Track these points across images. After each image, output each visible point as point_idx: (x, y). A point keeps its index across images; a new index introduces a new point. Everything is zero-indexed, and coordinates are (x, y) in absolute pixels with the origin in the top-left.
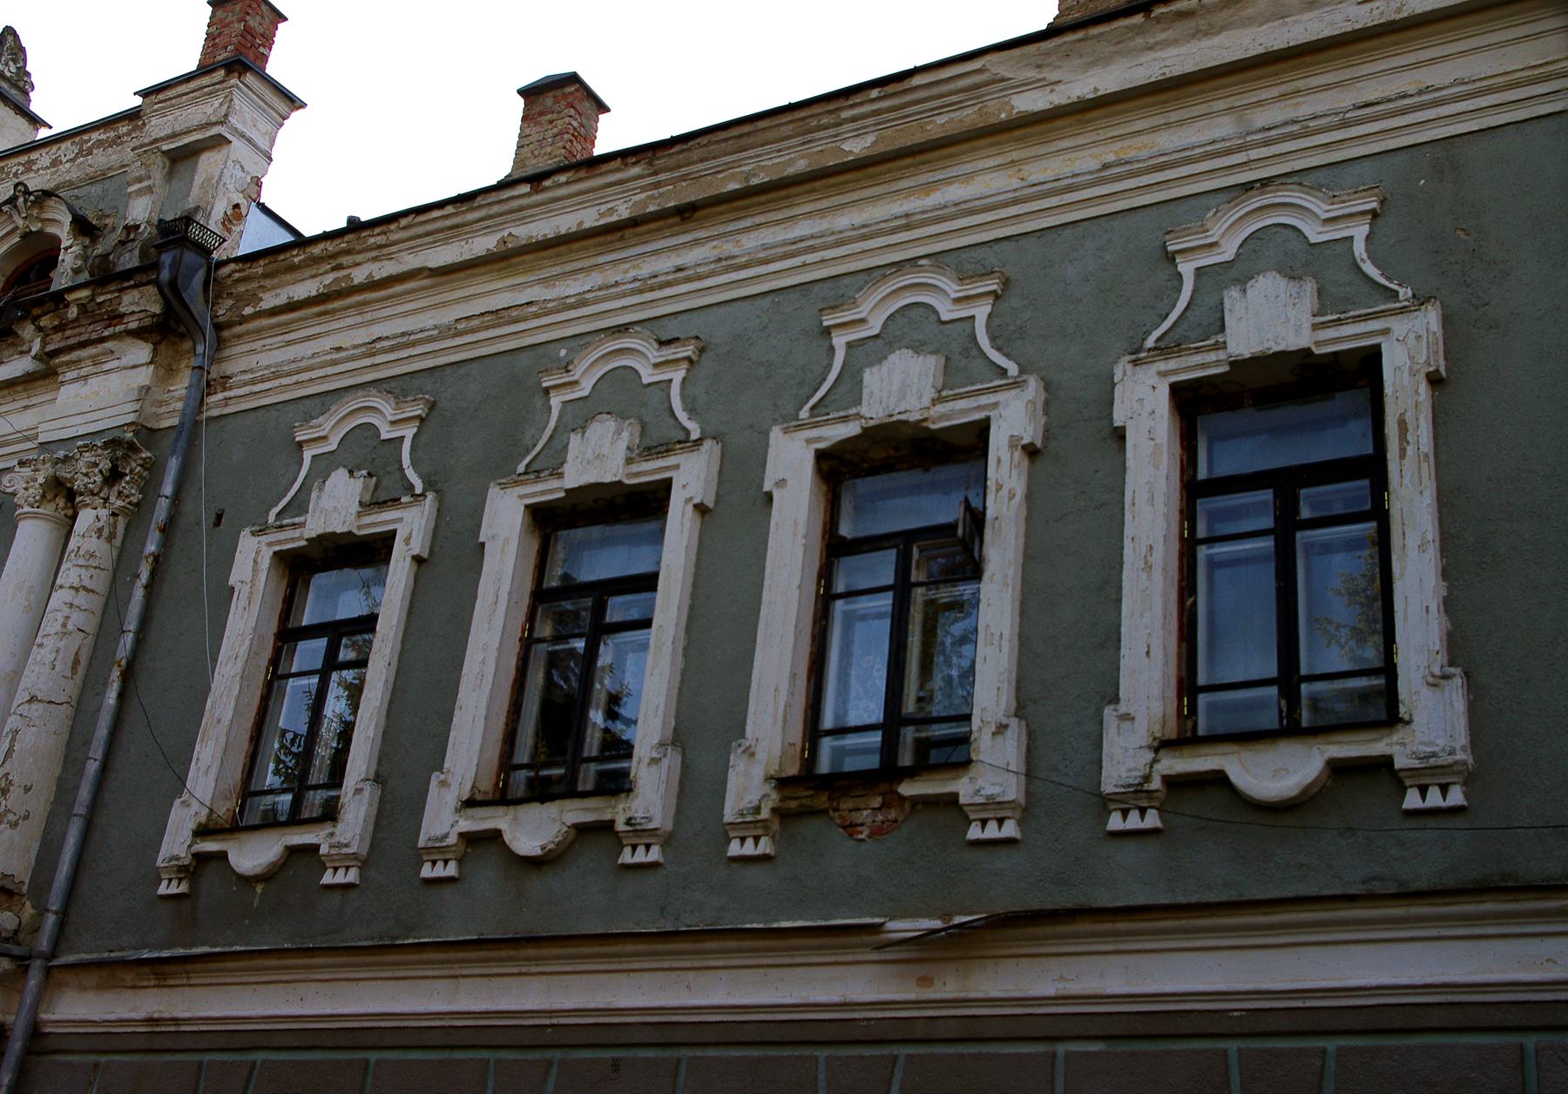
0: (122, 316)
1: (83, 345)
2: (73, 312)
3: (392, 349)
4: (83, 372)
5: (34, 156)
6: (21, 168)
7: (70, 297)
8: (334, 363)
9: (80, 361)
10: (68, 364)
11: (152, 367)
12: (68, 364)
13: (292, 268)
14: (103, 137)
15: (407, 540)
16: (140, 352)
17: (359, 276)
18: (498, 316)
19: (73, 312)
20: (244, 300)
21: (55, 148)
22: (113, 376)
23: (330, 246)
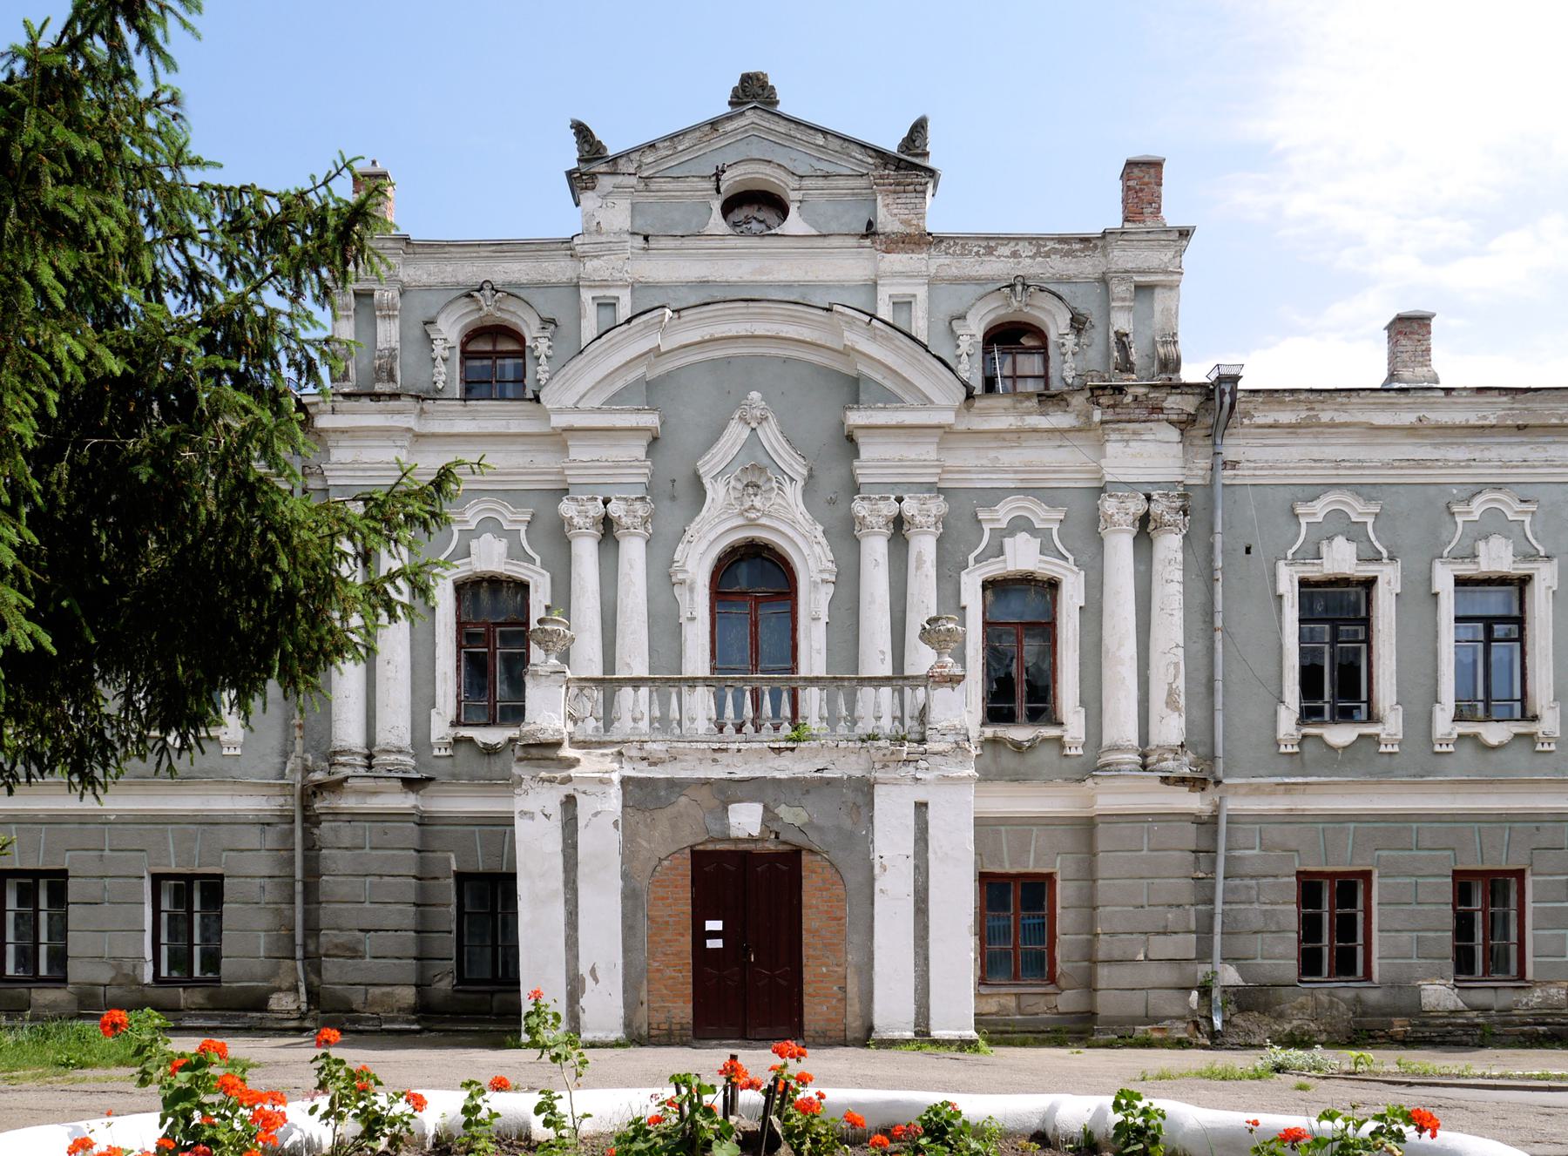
1: (1129, 421)
2: (1129, 399)
3: (1350, 468)
5: (992, 244)
8: (1312, 468)
10: (1114, 430)
13: (1281, 403)
15: (1389, 583)
16: (1174, 434)
17: (1325, 417)
18: (1419, 463)
19: (1129, 399)
20: (1247, 414)
21: (1012, 244)
23: (1312, 397)
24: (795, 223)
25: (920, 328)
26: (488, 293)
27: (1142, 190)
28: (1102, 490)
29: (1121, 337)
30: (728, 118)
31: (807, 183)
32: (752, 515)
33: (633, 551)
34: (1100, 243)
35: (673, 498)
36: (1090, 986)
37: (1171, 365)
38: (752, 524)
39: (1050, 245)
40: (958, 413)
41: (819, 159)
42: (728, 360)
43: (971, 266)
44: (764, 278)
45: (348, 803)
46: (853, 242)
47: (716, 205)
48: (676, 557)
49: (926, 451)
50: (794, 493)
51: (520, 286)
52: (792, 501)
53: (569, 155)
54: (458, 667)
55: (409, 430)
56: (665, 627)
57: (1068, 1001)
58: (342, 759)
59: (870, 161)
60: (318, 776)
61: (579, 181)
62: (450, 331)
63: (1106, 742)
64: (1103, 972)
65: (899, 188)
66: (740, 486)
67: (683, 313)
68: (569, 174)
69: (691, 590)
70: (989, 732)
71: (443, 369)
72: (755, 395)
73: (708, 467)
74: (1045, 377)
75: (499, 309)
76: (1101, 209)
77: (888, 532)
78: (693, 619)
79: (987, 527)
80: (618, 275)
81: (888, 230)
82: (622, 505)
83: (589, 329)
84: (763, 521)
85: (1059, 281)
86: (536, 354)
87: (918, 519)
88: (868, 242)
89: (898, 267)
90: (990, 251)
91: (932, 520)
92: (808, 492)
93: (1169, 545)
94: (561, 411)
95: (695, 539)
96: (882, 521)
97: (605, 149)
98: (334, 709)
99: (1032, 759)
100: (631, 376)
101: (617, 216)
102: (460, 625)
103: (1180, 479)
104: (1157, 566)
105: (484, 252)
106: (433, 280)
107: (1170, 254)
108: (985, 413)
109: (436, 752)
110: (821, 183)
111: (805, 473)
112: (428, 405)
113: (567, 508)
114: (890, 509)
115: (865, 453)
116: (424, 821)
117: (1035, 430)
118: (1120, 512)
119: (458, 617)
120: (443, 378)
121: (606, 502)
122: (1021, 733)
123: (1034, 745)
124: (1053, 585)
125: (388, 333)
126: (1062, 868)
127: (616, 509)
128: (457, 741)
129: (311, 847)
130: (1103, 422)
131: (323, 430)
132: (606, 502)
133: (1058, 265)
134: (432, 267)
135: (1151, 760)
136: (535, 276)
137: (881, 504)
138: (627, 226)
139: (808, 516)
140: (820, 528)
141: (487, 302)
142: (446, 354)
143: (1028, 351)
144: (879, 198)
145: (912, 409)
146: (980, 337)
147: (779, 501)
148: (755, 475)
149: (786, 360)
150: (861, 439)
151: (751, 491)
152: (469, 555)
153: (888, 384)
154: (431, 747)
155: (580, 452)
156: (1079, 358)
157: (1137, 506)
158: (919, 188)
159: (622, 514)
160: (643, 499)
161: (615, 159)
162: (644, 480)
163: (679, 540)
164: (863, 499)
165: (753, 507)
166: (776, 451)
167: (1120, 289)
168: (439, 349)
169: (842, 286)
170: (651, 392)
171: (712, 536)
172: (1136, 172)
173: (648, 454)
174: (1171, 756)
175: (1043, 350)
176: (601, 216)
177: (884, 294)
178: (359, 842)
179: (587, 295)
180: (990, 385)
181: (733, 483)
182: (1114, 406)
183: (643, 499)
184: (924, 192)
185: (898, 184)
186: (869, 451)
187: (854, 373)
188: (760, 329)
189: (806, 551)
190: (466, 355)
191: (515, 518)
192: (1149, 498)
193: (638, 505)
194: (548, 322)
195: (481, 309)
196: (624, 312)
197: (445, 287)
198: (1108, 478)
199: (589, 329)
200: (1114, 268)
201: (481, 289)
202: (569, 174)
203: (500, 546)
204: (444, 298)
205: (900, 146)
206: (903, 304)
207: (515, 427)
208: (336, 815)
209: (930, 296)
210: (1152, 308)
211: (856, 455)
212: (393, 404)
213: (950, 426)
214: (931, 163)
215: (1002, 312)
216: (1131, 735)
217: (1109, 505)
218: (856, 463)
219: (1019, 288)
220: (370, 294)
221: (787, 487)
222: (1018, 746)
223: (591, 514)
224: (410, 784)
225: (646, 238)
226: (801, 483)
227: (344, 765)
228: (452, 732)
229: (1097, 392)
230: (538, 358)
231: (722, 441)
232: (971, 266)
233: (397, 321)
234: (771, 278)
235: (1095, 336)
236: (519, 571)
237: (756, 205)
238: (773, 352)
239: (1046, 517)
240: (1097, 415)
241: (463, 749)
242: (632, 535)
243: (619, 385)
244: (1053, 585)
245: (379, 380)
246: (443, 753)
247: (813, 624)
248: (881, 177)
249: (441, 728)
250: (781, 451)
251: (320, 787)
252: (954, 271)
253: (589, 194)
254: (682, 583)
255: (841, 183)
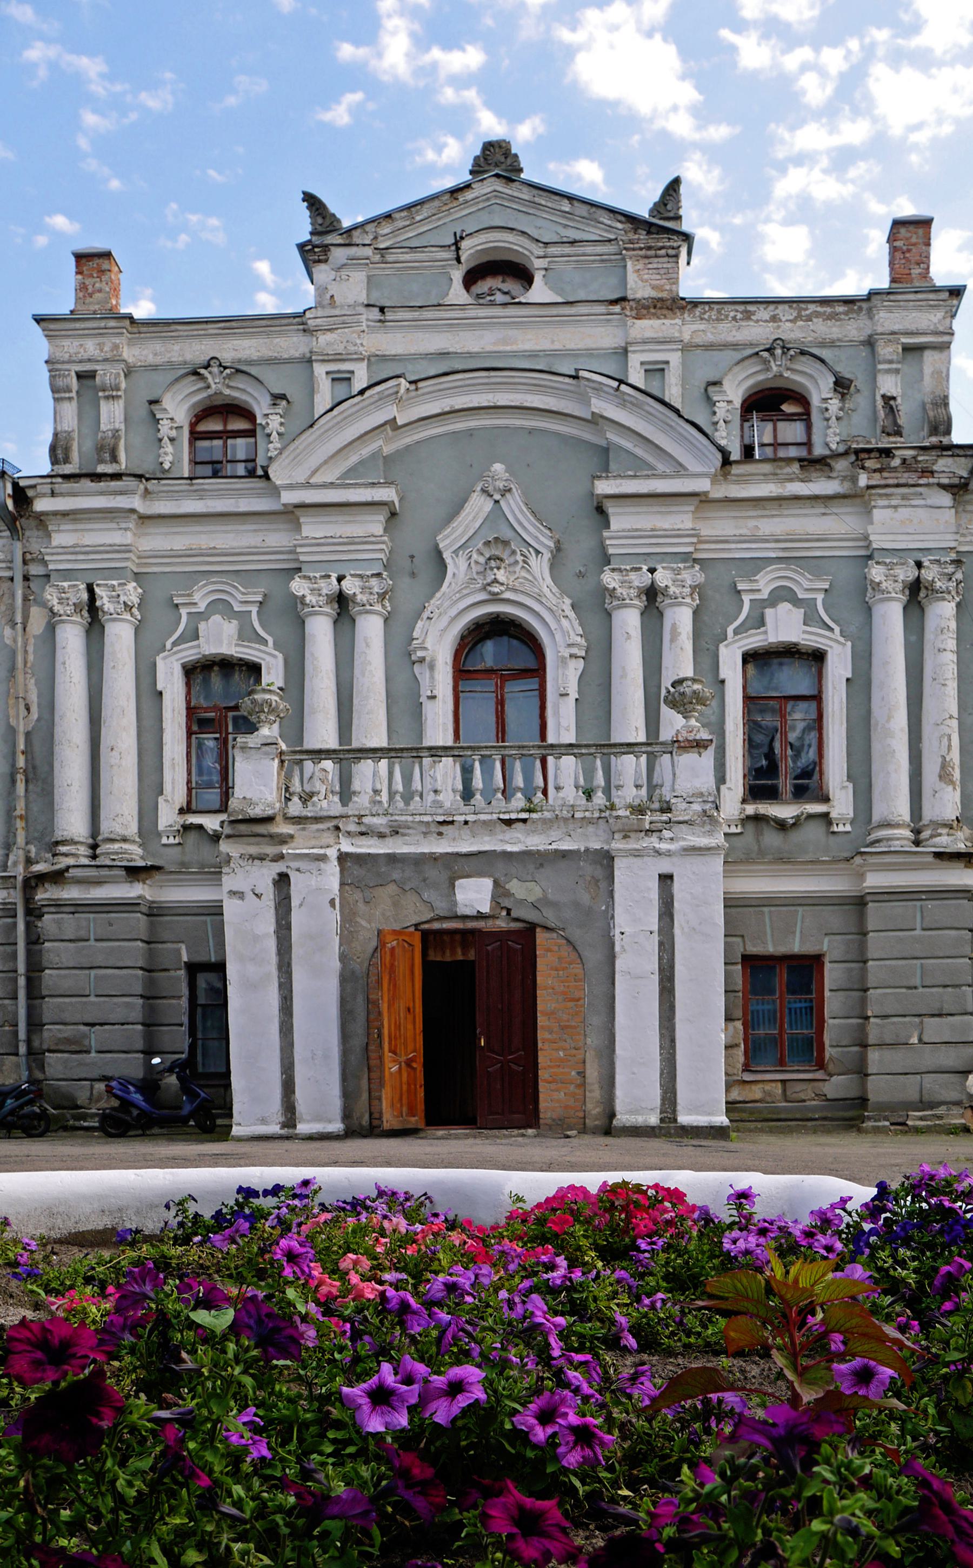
0: (932, 472)
1: (898, 486)
2: (896, 462)
4: (894, 502)
5: (751, 308)
6: (739, 316)
7: (897, 453)
9: (891, 495)
10: (880, 495)
11: (953, 510)
12: (880, 495)
14: (819, 309)
16: (946, 499)
19: (896, 462)
21: (772, 307)
22: (919, 510)
24: (539, 292)
25: (673, 394)
26: (215, 370)
27: (909, 251)
28: (870, 557)
29: (888, 399)
30: (468, 186)
31: (552, 250)
32: (496, 589)
33: (371, 629)
34: (865, 305)
35: (413, 575)
36: (862, 1072)
37: (942, 426)
38: (495, 598)
39: (812, 307)
40: (714, 480)
41: (566, 226)
42: (470, 433)
43: (727, 332)
44: (508, 348)
45: (71, 893)
46: (601, 309)
47: (458, 275)
48: (415, 635)
49: (681, 519)
50: (540, 566)
51: (250, 363)
52: (538, 575)
53: (302, 228)
54: (188, 754)
55: (133, 511)
56: (406, 703)
57: (838, 1085)
58: (63, 849)
59: (620, 226)
60: (40, 868)
61: (312, 254)
62: (178, 409)
63: (876, 818)
64: (874, 1056)
65: (650, 253)
66: (482, 560)
67: (420, 384)
68: (301, 247)
69: (432, 667)
70: (750, 809)
71: (169, 448)
72: (498, 467)
73: (447, 542)
74: (808, 444)
75: (228, 387)
76: (866, 272)
77: (640, 603)
78: (433, 697)
79: (746, 598)
80: (352, 349)
81: (639, 295)
82: (358, 582)
83: (323, 399)
84: (507, 595)
85: (822, 344)
86: (268, 431)
87: (672, 590)
88: (617, 309)
89: (649, 334)
90: (748, 316)
91: (687, 590)
92: (554, 565)
93: (943, 613)
94: (291, 487)
95: (435, 616)
96: (633, 593)
97: (339, 221)
98: (56, 798)
99: (796, 837)
100: (366, 451)
101: (353, 289)
102: (191, 711)
103: (953, 544)
104: (929, 636)
105: (212, 329)
106: (159, 360)
107: (940, 315)
108: (743, 480)
109: (164, 840)
110: (567, 250)
111: (552, 545)
112: (151, 485)
113: (298, 586)
114: (641, 579)
115: (615, 524)
116: (155, 912)
117: (797, 498)
118: (890, 579)
119: (188, 702)
120: (170, 458)
121: (340, 579)
122: (785, 811)
123: (797, 822)
124: (818, 657)
125: (112, 415)
126: (831, 948)
127: (350, 586)
128: (187, 828)
129: (34, 940)
130: (869, 487)
131: (43, 513)
132: (340, 579)
133: (822, 329)
134: (158, 346)
135: (925, 835)
136: (267, 353)
137: (633, 576)
138: (363, 299)
139: (555, 589)
140: (568, 601)
141: (215, 381)
142: (173, 433)
143: (790, 418)
144: (629, 264)
145: (664, 476)
146: (738, 403)
147: (524, 574)
148: (498, 547)
149: (531, 431)
150: (611, 509)
151: (493, 564)
152: (197, 638)
153: (639, 452)
154: (159, 835)
155: (313, 528)
156: (844, 422)
157: (907, 573)
158: (671, 252)
159: (358, 591)
160: (378, 575)
161: (350, 231)
162: (381, 556)
163: (419, 616)
164: (613, 570)
165: (495, 581)
166: (520, 524)
167: (886, 350)
168: (165, 429)
169: (590, 353)
170: (388, 467)
171: (453, 612)
172: (903, 231)
173: (385, 530)
174: (944, 831)
175: (805, 417)
176: (334, 289)
177: (635, 360)
178: (82, 934)
179: (320, 370)
180: (748, 451)
181: (475, 556)
182: (880, 470)
183: (378, 575)
184: (677, 256)
185: (649, 248)
186: (620, 520)
187: (603, 443)
188: (503, 399)
189: (553, 625)
190: (195, 436)
191: (245, 598)
192: (919, 565)
193: (374, 582)
194: (278, 398)
195: (209, 387)
196: (360, 382)
197: (171, 365)
198: (875, 546)
199: (323, 399)
200: (880, 330)
201: (207, 366)
202: (301, 247)
203: (230, 628)
204: (171, 376)
205: (651, 211)
206: (656, 370)
207: (244, 505)
208: (58, 905)
209: (684, 363)
210: (921, 371)
211: (607, 525)
212: (114, 484)
213: (706, 493)
214: (685, 227)
215: (761, 377)
216: (902, 809)
217: (876, 573)
218: (605, 534)
219: (778, 352)
220: (92, 375)
221: (533, 560)
222: (781, 825)
223: (324, 591)
224: (134, 873)
225: (382, 310)
226: (547, 555)
227: (66, 855)
228: (181, 820)
229: (863, 456)
230: (269, 435)
231: (463, 514)
232: (727, 332)
233: (121, 402)
234: (514, 348)
235: (860, 401)
236: (250, 653)
237: (501, 271)
238: (518, 423)
239: (806, 585)
240: (863, 480)
241: (192, 837)
242: (368, 612)
243: (354, 459)
244: (818, 657)
245: (101, 461)
246: (171, 840)
247: (562, 700)
248: (631, 242)
249: (168, 817)
250: (526, 524)
251: (42, 878)
252: (710, 337)
253: (322, 267)
254: (422, 660)
255: (589, 249)
